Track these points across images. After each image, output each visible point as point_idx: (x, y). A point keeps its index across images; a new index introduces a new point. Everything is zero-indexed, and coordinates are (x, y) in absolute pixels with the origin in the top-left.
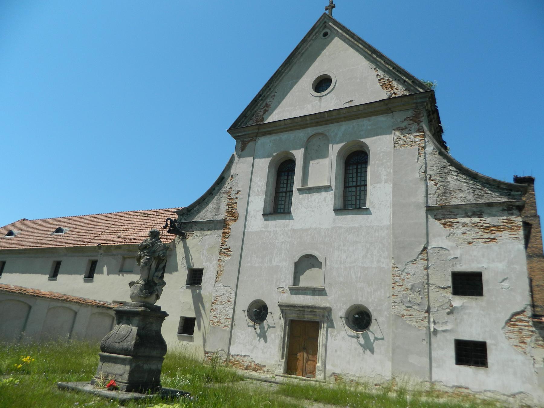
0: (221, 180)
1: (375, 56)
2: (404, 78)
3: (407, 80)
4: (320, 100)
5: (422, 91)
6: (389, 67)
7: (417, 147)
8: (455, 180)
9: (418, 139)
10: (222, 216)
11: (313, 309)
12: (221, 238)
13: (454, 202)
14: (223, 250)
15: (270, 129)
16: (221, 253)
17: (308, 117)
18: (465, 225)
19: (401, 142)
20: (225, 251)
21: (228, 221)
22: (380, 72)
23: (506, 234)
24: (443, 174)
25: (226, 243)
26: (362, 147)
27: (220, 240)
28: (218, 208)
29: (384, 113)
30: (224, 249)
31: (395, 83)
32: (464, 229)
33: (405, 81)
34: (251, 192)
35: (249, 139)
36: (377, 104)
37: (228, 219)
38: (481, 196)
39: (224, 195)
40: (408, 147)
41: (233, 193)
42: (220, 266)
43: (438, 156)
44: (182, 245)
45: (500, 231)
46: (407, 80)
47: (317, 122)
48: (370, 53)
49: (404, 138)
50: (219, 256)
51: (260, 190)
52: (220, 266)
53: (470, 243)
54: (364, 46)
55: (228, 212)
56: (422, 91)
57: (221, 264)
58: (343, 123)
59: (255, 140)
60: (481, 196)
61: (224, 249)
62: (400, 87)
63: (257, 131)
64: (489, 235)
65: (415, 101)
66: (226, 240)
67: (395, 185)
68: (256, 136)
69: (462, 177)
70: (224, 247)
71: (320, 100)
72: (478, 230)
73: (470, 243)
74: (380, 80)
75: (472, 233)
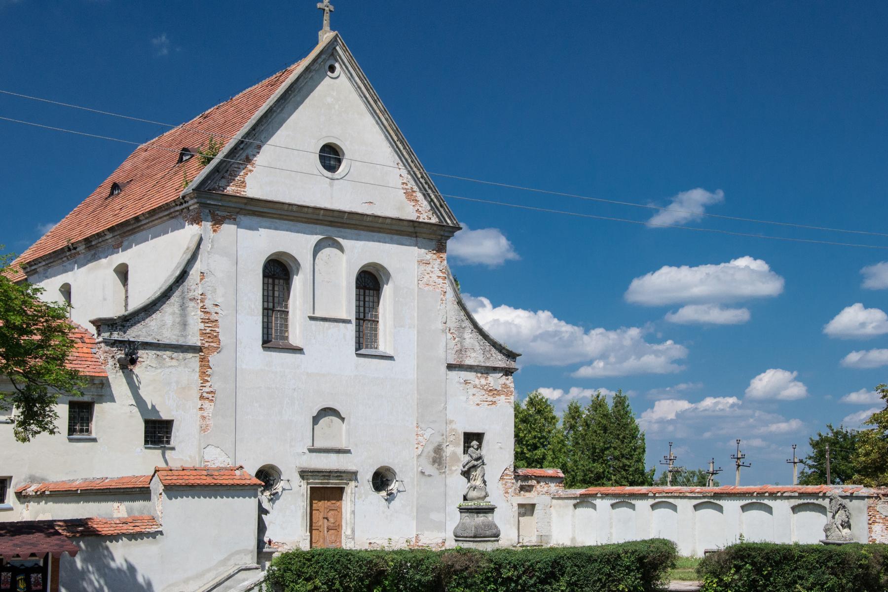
0: (183, 276)
1: (402, 148)
2: (433, 197)
3: (435, 200)
4: (331, 185)
5: (449, 221)
6: (418, 173)
7: (439, 291)
8: (470, 338)
9: (441, 281)
10: (195, 340)
11: (339, 474)
12: (198, 374)
13: (469, 362)
14: (205, 394)
15: (265, 210)
16: (202, 398)
17: (322, 212)
18: (475, 386)
19: (425, 280)
20: (210, 396)
21: (207, 348)
22: (404, 172)
23: (503, 397)
24: (461, 329)
25: (208, 384)
26: (378, 270)
27: (196, 376)
28: (184, 325)
29: (408, 235)
30: (207, 393)
31: (420, 196)
32: (474, 391)
33: (432, 200)
34: (239, 308)
35: (225, 214)
36: (405, 223)
37: (207, 345)
38: (489, 358)
39: (192, 304)
40: (431, 288)
41: (208, 304)
42: (204, 418)
43: (456, 306)
44: (124, 380)
45: (499, 395)
46: (435, 200)
47: (331, 222)
48: (396, 138)
49: (428, 276)
50: (200, 403)
51: (253, 306)
52: (204, 418)
53: (478, 405)
54: (390, 125)
55: (203, 333)
56: (449, 221)
57: (205, 414)
58: (362, 232)
59: (235, 219)
60: (489, 358)
61: (207, 393)
62: (425, 203)
63: (243, 206)
64: (490, 399)
65: (442, 233)
66: (209, 379)
67: (418, 332)
68: (238, 213)
69: (476, 335)
70: (207, 389)
71: (331, 185)
72: (484, 392)
73: (478, 405)
74: (403, 183)
75: (481, 395)
